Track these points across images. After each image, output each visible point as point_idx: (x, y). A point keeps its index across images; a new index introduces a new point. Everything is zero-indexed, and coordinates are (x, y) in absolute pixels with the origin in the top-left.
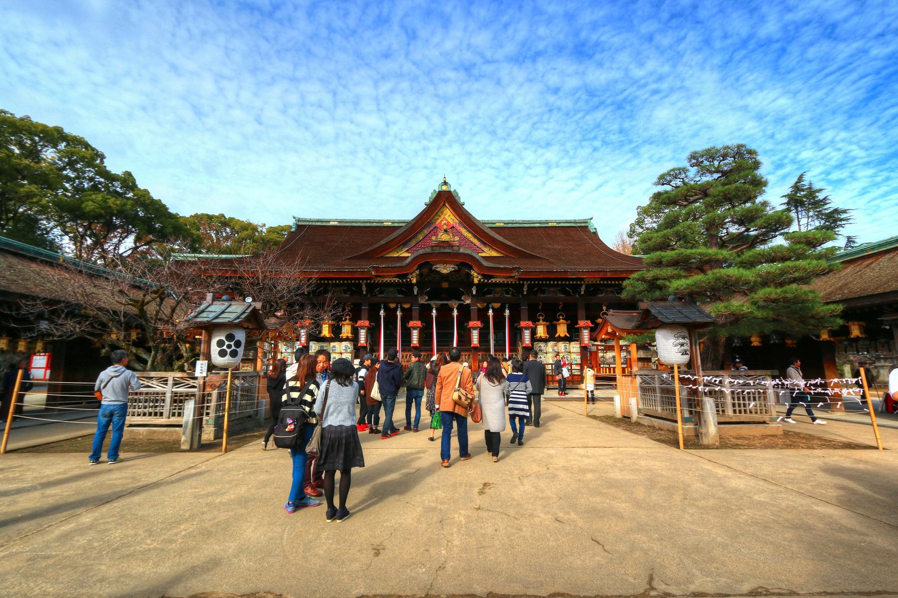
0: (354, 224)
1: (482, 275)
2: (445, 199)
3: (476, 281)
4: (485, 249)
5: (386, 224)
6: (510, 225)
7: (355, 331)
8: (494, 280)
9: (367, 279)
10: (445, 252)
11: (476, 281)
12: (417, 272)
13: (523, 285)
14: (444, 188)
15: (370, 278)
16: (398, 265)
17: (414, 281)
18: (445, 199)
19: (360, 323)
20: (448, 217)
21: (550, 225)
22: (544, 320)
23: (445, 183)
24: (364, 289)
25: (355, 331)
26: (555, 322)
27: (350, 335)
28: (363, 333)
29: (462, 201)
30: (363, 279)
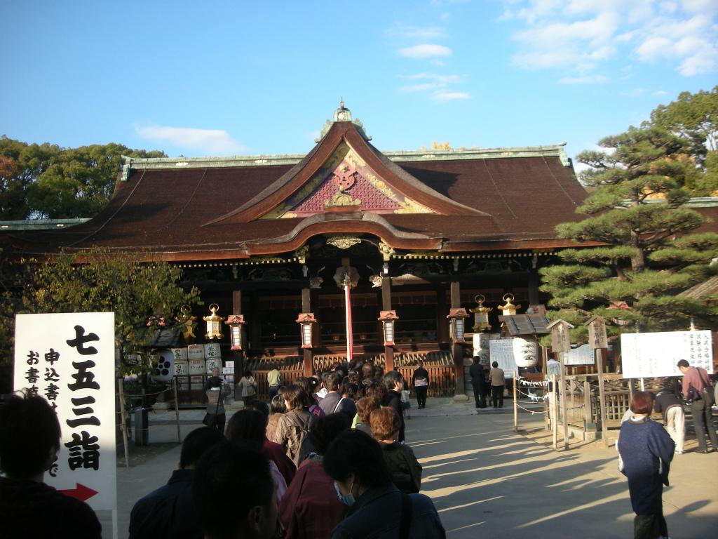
0: (212, 165)
1: (394, 249)
2: (345, 135)
3: (386, 258)
4: (403, 204)
5: (259, 163)
6: (444, 158)
7: (225, 330)
8: (410, 256)
9: (238, 260)
10: (345, 220)
11: (386, 258)
12: (306, 248)
13: (452, 261)
14: (342, 117)
15: (243, 260)
16: (280, 241)
17: (302, 261)
18: (345, 135)
19: (231, 319)
20: (353, 159)
21: (504, 155)
22: (484, 305)
23: (344, 109)
24: (235, 272)
25: (225, 330)
26: (500, 307)
27: (218, 335)
28: (236, 333)
29: (368, 135)
30: (233, 261)
